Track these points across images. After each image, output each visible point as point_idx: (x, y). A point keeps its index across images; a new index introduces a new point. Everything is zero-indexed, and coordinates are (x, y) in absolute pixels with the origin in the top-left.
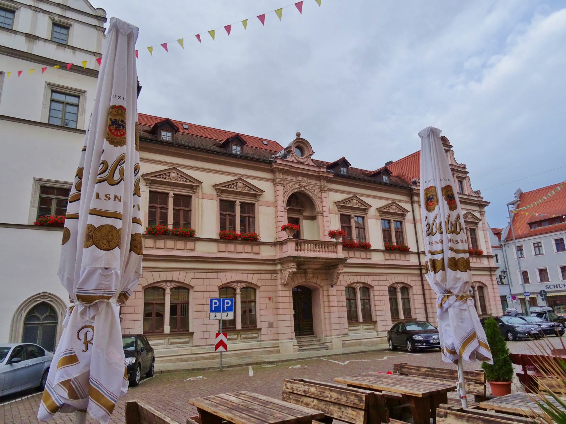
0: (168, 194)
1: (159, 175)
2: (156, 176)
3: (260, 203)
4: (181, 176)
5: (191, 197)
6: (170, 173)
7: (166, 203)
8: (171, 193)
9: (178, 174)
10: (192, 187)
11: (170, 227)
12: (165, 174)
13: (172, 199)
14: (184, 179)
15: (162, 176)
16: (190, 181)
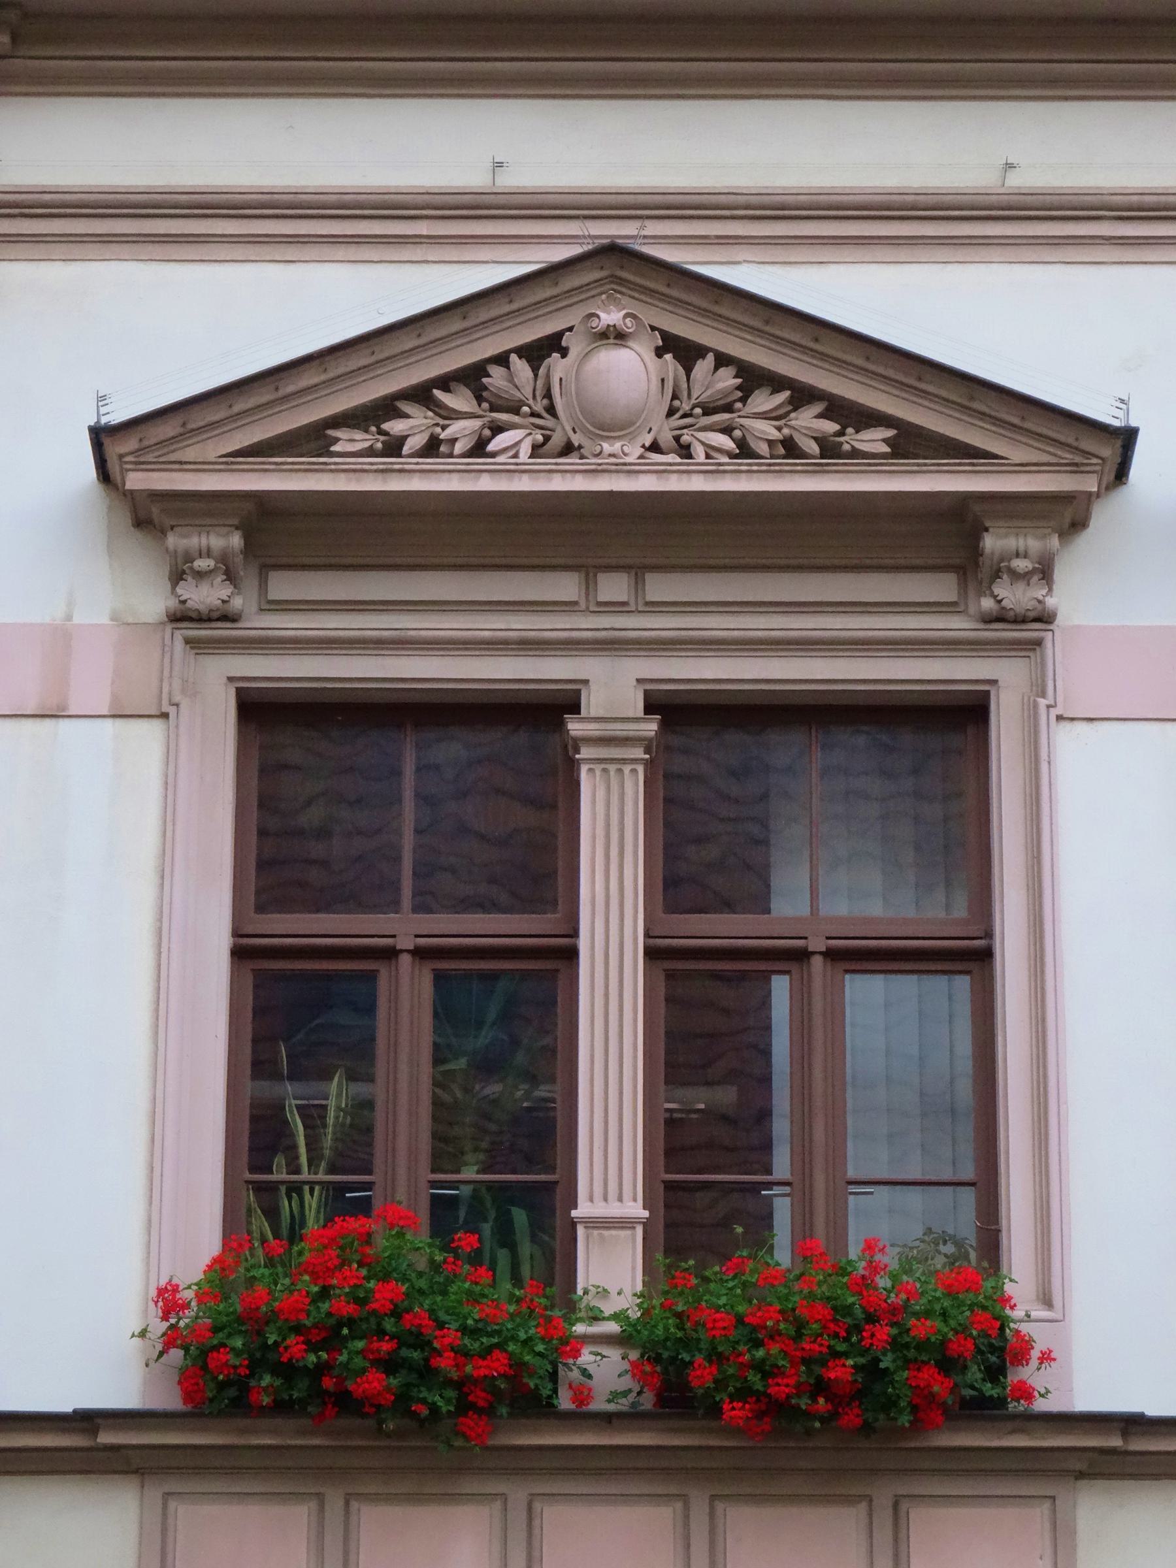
0: (568, 702)
1: (387, 408)
2: (313, 441)
3: (1071, 661)
4: (753, 379)
5: (968, 713)
6: (539, 352)
7: (542, 871)
8: (613, 692)
9: (684, 352)
10: (950, 538)
11: (612, 1272)
12: (472, 377)
13: (634, 785)
14: (809, 423)
15: (414, 425)
16: (911, 444)
